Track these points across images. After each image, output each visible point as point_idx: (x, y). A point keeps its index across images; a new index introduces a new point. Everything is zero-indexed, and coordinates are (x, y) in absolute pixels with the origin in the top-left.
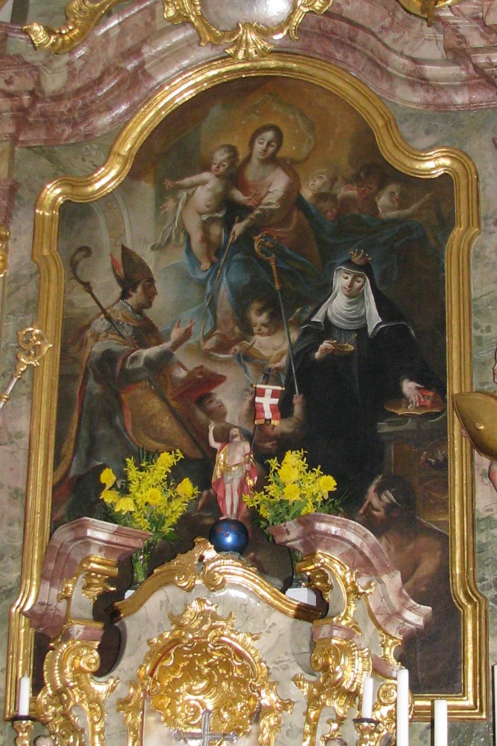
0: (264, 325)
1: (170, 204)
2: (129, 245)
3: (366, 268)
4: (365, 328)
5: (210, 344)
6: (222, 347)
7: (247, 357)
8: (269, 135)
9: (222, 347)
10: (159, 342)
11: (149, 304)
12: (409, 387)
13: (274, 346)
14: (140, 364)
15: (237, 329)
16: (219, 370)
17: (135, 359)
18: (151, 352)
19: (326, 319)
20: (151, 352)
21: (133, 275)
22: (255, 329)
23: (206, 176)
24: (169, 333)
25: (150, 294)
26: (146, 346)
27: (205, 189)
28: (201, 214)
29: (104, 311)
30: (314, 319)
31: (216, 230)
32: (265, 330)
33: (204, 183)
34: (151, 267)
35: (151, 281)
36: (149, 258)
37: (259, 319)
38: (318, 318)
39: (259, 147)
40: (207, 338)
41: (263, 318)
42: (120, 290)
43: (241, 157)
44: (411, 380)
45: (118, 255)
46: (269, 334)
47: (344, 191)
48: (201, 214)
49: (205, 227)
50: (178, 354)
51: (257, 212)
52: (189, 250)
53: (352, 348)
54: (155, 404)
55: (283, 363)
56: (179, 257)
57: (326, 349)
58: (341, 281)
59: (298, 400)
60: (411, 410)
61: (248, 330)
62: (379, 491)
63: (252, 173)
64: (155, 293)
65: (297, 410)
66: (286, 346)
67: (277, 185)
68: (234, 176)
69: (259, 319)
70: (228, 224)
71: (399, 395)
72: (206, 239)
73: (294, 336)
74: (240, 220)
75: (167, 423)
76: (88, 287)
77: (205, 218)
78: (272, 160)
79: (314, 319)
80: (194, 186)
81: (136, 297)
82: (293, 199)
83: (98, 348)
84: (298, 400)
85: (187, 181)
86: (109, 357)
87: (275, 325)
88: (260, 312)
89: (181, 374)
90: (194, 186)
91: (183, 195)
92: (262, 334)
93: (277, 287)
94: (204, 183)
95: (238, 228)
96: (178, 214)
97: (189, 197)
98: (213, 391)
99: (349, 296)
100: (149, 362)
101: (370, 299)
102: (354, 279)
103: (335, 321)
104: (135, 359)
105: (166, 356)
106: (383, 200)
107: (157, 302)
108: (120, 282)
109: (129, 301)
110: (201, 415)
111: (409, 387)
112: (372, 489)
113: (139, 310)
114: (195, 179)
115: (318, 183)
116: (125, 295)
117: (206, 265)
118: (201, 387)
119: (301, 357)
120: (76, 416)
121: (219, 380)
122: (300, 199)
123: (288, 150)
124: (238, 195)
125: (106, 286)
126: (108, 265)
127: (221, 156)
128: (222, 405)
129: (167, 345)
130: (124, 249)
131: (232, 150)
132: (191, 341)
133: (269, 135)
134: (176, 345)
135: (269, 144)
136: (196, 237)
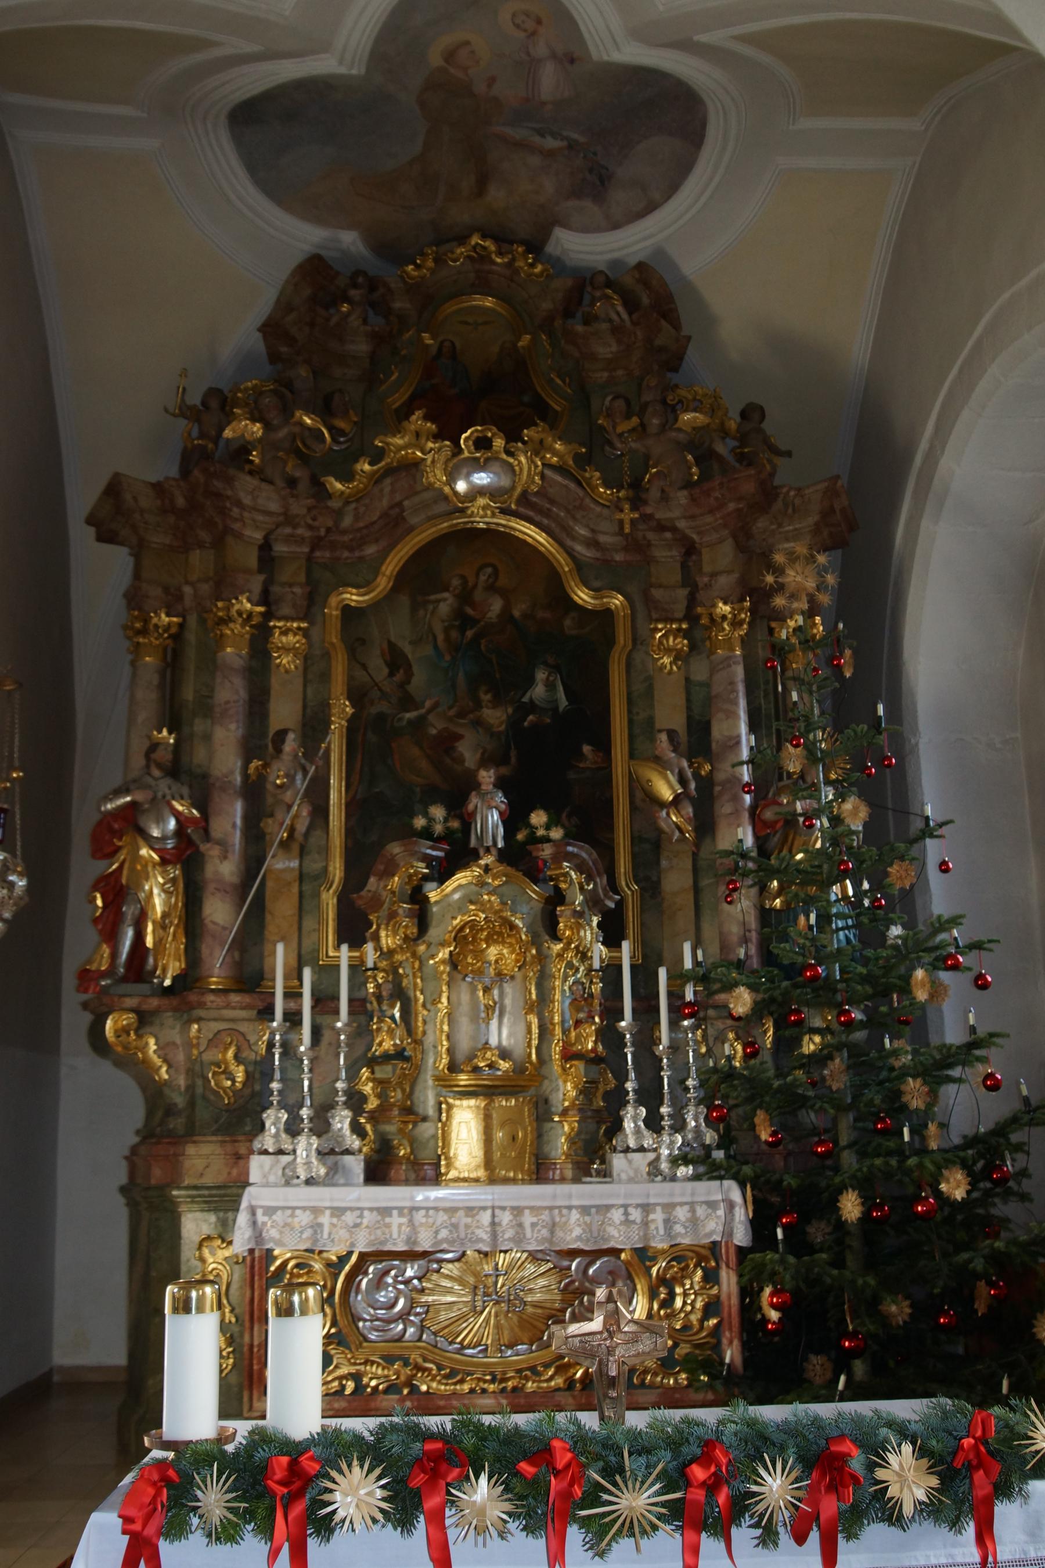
0: (490, 701)
1: (421, 612)
2: (393, 639)
3: (556, 668)
4: (557, 708)
5: (452, 713)
6: (461, 715)
7: (478, 723)
8: (489, 570)
9: (461, 715)
10: (417, 709)
11: (409, 683)
12: (586, 749)
13: (496, 716)
14: (404, 723)
15: (471, 704)
16: (461, 731)
17: (400, 719)
19: (531, 700)
21: (396, 661)
22: (484, 704)
23: (446, 595)
24: (424, 702)
25: (409, 674)
26: (408, 711)
27: (445, 605)
28: (443, 621)
29: (377, 685)
30: (523, 700)
31: (454, 634)
32: (490, 705)
33: (445, 600)
34: (410, 656)
35: (410, 666)
36: (408, 649)
38: (525, 699)
39: (483, 578)
40: (450, 708)
41: (489, 697)
42: (386, 671)
43: (470, 584)
44: (589, 744)
45: (385, 646)
46: (494, 708)
47: (541, 614)
48: (443, 621)
49: (446, 630)
50: (431, 718)
51: (482, 623)
52: (436, 647)
53: (548, 721)
54: (416, 751)
55: (503, 728)
56: (428, 650)
57: (532, 721)
58: (541, 675)
59: (513, 754)
60: (588, 764)
61: (478, 705)
62: (569, 816)
63: (478, 595)
64: (412, 674)
65: (513, 760)
66: (504, 717)
67: (496, 605)
68: (465, 597)
70: (462, 630)
71: (581, 756)
72: (447, 639)
73: (510, 710)
74: (471, 628)
75: (424, 764)
76: (364, 667)
77: (446, 624)
78: (491, 588)
79: (523, 700)
80: (438, 601)
81: (399, 676)
82: (506, 614)
83: (374, 710)
84: (513, 754)
85: (433, 597)
86: (381, 717)
87: (497, 702)
88: (486, 693)
89: (434, 732)
90: (438, 601)
91: (431, 607)
92: (488, 708)
93: (498, 676)
94: (445, 600)
95: (469, 634)
96: (427, 620)
97: (435, 608)
98: (457, 744)
99: (546, 686)
100: (410, 722)
101: (561, 688)
102: (549, 675)
103: (537, 702)
104: (400, 719)
105: (422, 719)
106: (567, 622)
107: (415, 680)
108: (388, 665)
109: (394, 679)
110: (448, 761)
111: (586, 749)
112: (564, 815)
113: (402, 685)
114: (438, 596)
115: (524, 606)
116: (391, 674)
117: (448, 658)
118: (447, 742)
119: (515, 723)
120: (359, 757)
121: (460, 737)
122: (512, 616)
123: (503, 581)
124: (469, 611)
125: (378, 668)
126: (378, 652)
127: (456, 582)
128: (462, 755)
129: (423, 711)
130: (389, 642)
131: (463, 577)
132: (440, 709)
133: (489, 570)
134: (429, 712)
135: (489, 576)
136: (440, 637)
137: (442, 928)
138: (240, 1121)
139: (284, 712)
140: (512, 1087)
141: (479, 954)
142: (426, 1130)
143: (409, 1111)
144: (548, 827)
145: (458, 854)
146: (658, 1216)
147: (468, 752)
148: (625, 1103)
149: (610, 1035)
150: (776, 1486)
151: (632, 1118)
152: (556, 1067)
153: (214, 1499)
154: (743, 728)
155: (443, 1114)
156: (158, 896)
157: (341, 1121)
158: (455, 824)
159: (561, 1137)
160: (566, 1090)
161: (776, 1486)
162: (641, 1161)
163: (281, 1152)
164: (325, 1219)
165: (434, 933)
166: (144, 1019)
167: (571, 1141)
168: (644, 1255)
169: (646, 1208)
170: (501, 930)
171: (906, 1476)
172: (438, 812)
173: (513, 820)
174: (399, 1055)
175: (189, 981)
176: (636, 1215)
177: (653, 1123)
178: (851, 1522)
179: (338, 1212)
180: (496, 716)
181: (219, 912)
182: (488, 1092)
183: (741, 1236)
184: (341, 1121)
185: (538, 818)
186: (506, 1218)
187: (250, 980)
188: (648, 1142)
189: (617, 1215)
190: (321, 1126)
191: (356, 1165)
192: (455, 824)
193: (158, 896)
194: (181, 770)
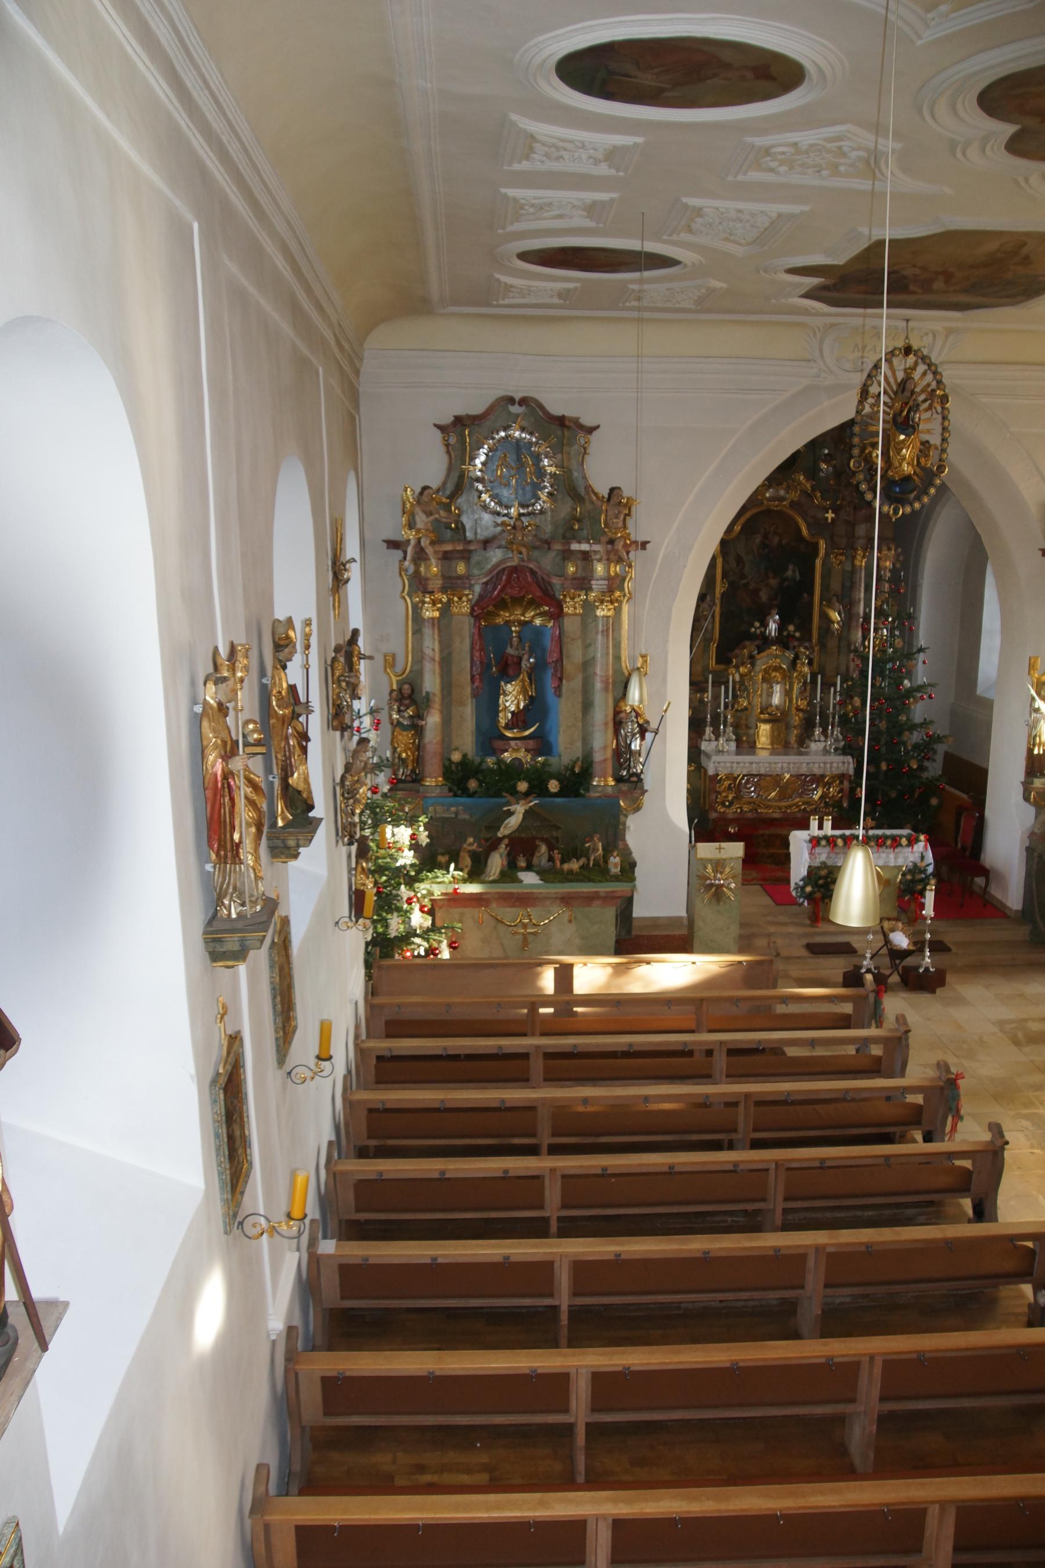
12: (805, 595)
13: (774, 582)
18: (744, 581)
20: (744, 581)
27: (758, 539)
37: (771, 575)
58: (791, 567)
67: (776, 540)
68: (765, 537)
69: (771, 575)
111: (805, 595)
118: (756, 592)
121: (760, 590)
127: (762, 531)
140: (778, 719)
141: (770, 675)
142: (751, 731)
143: (748, 727)
144: (795, 632)
145: (765, 642)
146: (828, 766)
147: (764, 596)
148: (814, 726)
149: (810, 704)
150: (889, 842)
151: (817, 731)
152: (794, 711)
153: (823, 843)
154: (862, 595)
158: (763, 629)
159: (793, 735)
160: (796, 719)
161: (889, 842)
162: (820, 746)
163: (710, 740)
164: (735, 765)
165: (757, 668)
167: (796, 736)
168: (823, 776)
169: (825, 763)
170: (777, 669)
171: (904, 841)
172: (757, 624)
173: (781, 628)
174: (746, 709)
176: (822, 765)
177: (824, 732)
178: (897, 846)
179: (738, 763)
180: (774, 582)
185: (791, 628)
186: (785, 765)
188: (822, 738)
189: (817, 765)
192: (763, 629)
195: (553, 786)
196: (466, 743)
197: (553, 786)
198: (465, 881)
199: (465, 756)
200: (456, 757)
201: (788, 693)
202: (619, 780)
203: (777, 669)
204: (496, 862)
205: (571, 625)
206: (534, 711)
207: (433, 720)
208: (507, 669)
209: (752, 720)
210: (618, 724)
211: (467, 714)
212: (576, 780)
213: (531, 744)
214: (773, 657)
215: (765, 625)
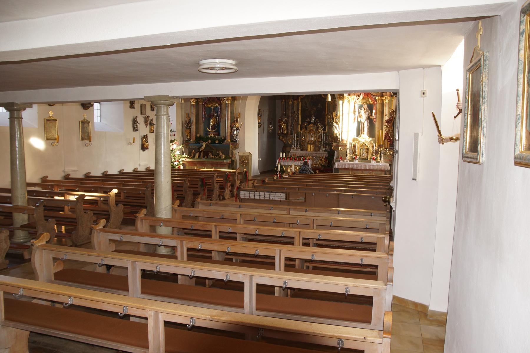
137: (308, 129)
138: (291, 146)
139: (295, 109)
140: (313, 143)
145: (310, 123)
147: (312, 112)
155: (307, 146)
156: (284, 126)
157: (299, 146)
166: (283, 137)
175: (287, 133)
180: (315, 109)
181: (290, 128)
182: (311, 144)
183: (327, 156)
184: (299, 146)
187: (292, 134)
190: (297, 146)
191: (299, 150)
193: (284, 126)
194: (286, 115)
195: (217, 142)
196: (201, 133)
197: (217, 142)
198: (188, 158)
199: (200, 136)
200: (198, 135)
201: (316, 137)
202: (232, 141)
203: (313, 130)
204: (197, 155)
205: (223, 106)
206: (217, 127)
207: (193, 127)
208: (210, 117)
209: (306, 144)
210: (232, 128)
211: (202, 126)
212: (222, 141)
213: (215, 133)
214: (311, 127)
215: (311, 120)
